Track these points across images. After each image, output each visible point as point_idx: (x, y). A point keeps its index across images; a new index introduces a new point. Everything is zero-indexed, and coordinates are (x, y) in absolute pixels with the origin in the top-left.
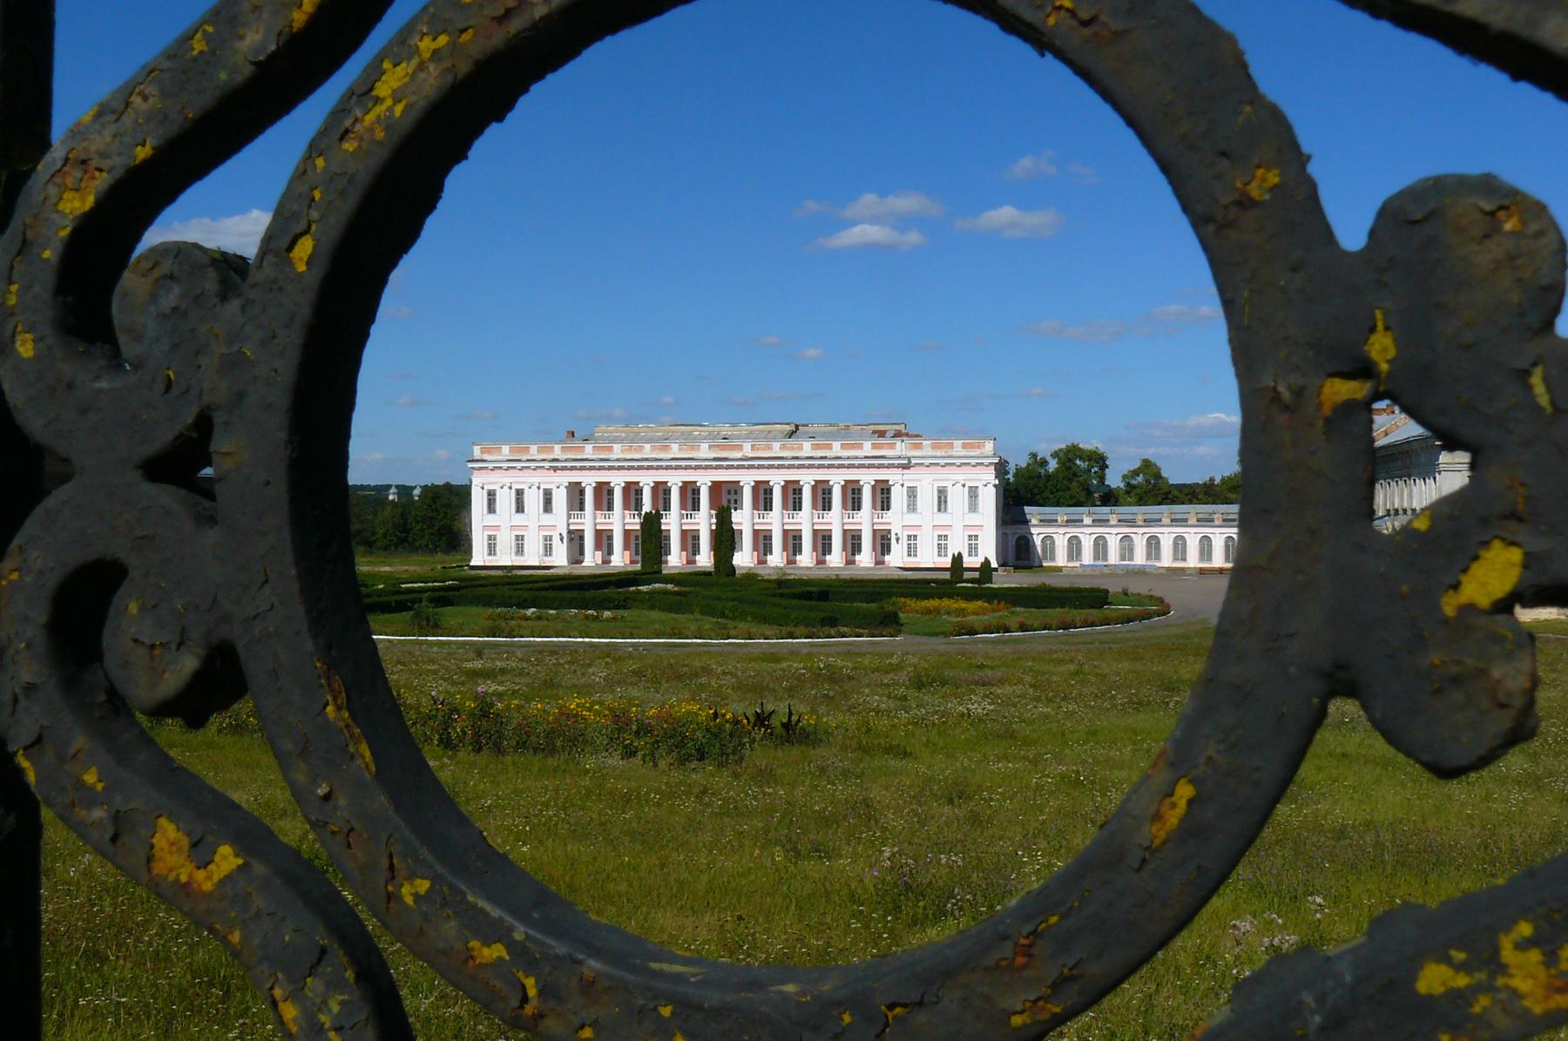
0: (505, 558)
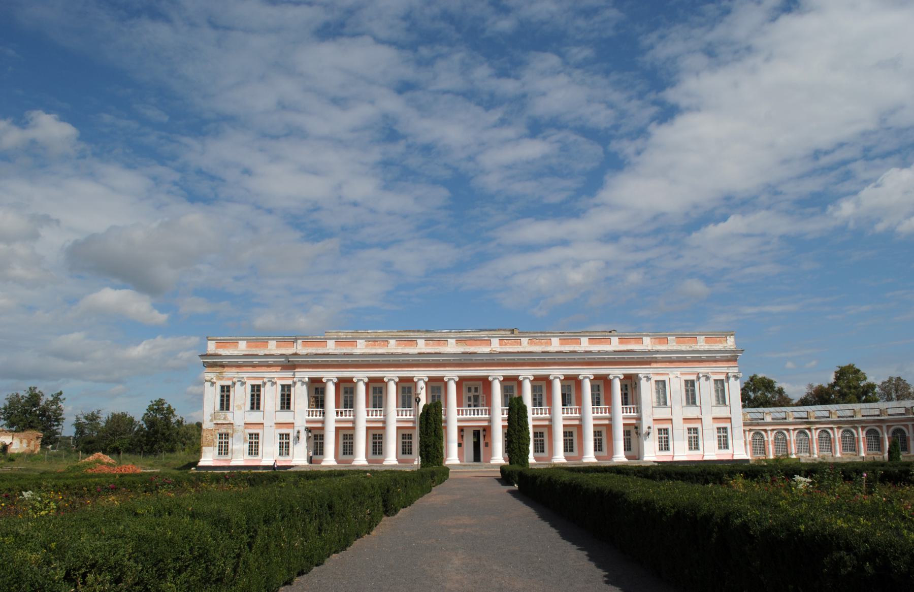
0: (240, 457)
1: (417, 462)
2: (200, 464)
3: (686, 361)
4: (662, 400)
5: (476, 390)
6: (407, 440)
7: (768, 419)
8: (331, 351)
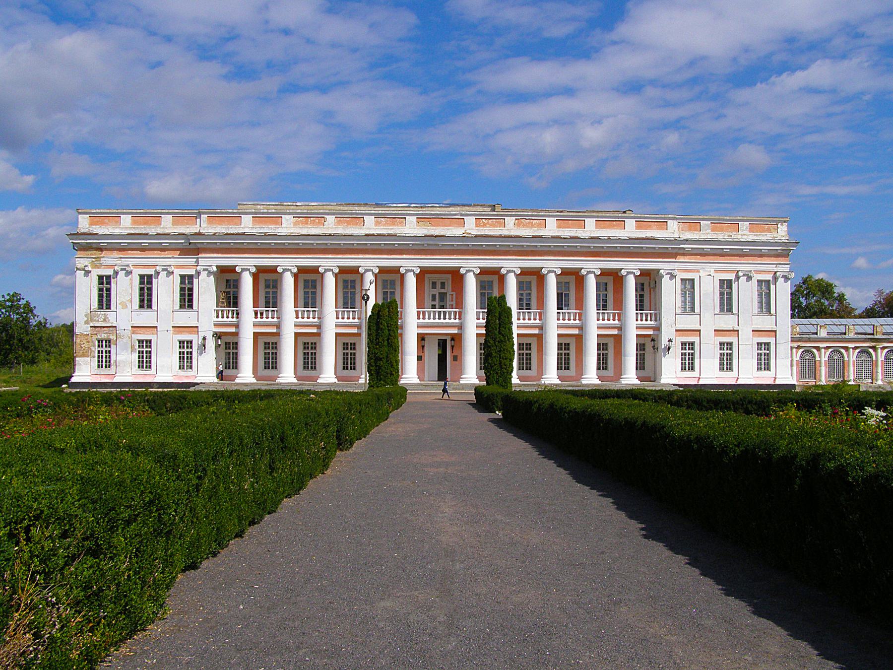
0: (126, 371)
1: (363, 379)
2: (73, 380)
3: (722, 254)
4: (688, 305)
5: (443, 285)
6: (349, 351)
7: (823, 334)
8: (247, 231)
